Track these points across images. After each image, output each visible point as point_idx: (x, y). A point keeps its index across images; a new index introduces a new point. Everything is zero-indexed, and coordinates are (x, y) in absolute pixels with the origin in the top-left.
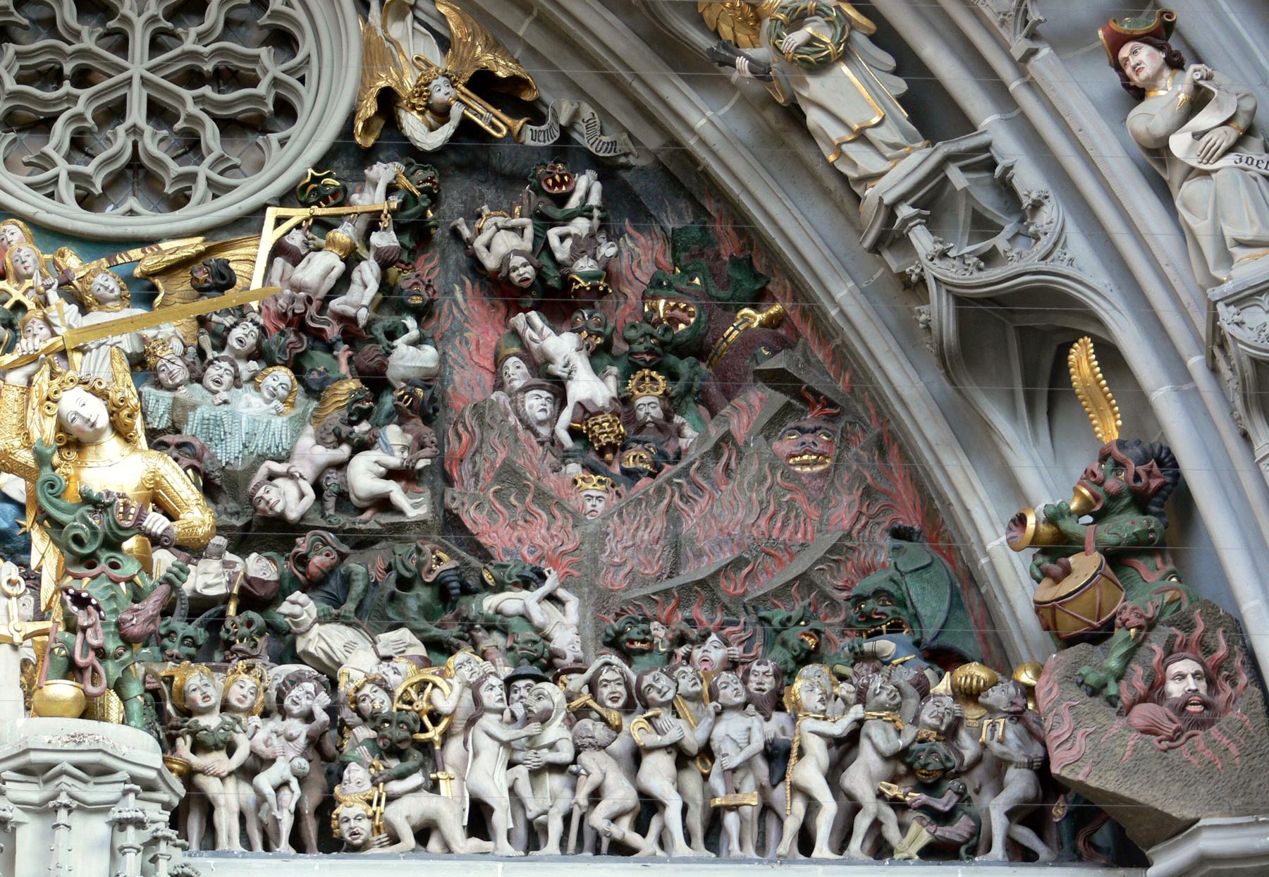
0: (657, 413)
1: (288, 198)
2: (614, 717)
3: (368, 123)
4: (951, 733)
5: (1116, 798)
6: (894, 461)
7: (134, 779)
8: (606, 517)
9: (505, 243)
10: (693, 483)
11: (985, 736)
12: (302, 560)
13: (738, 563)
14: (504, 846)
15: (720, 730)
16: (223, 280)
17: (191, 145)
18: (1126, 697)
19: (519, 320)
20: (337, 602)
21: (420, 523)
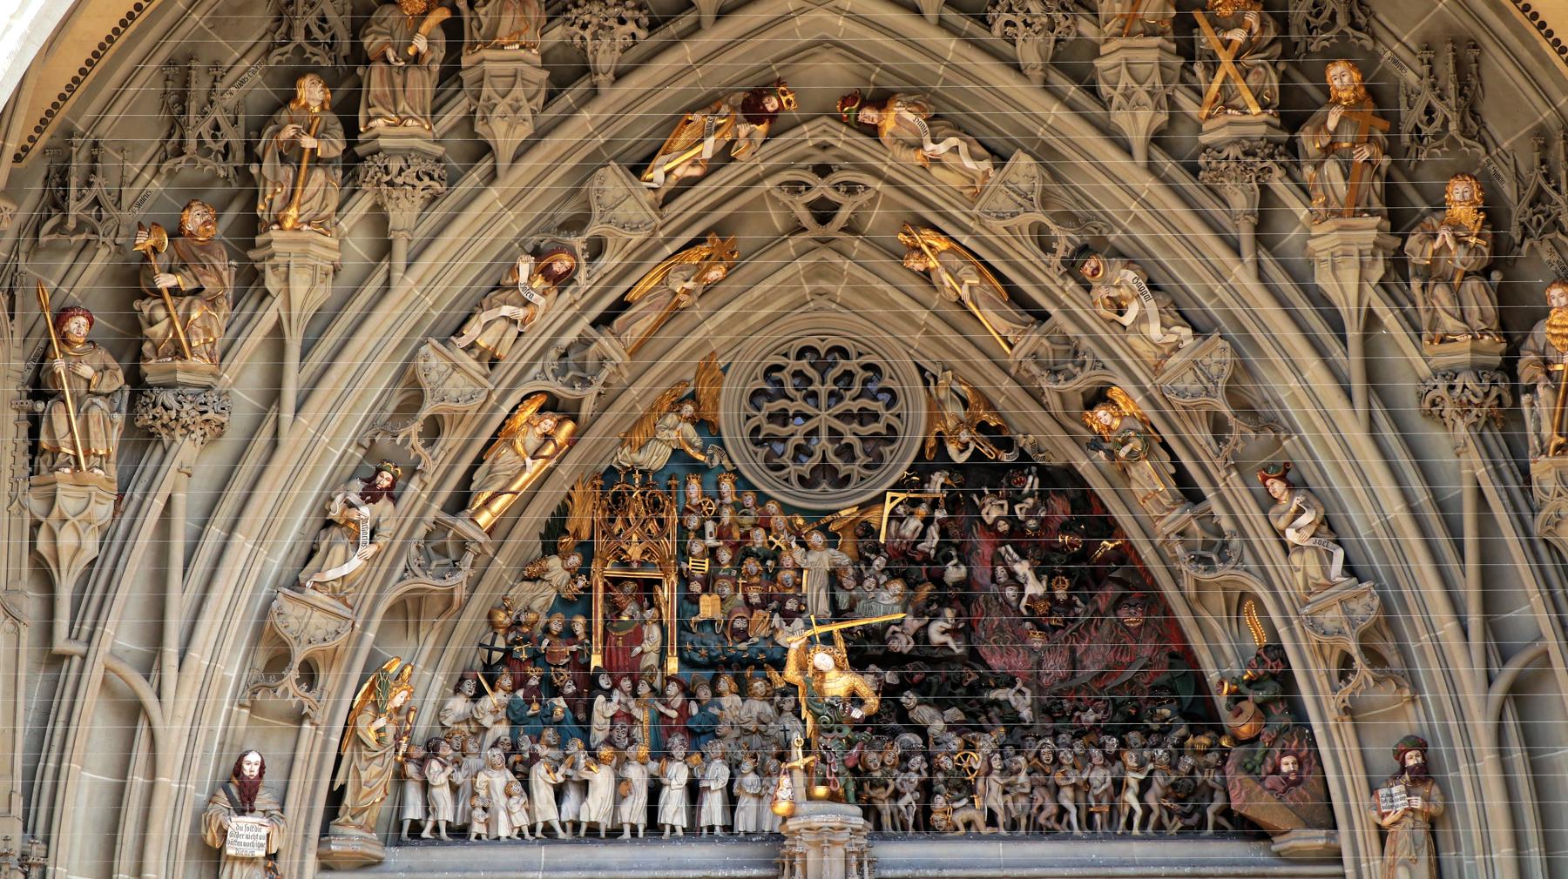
1: (896, 487)
2: (1048, 770)
3: (931, 449)
9: (995, 514)
16: (870, 531)
21: (960, 656)
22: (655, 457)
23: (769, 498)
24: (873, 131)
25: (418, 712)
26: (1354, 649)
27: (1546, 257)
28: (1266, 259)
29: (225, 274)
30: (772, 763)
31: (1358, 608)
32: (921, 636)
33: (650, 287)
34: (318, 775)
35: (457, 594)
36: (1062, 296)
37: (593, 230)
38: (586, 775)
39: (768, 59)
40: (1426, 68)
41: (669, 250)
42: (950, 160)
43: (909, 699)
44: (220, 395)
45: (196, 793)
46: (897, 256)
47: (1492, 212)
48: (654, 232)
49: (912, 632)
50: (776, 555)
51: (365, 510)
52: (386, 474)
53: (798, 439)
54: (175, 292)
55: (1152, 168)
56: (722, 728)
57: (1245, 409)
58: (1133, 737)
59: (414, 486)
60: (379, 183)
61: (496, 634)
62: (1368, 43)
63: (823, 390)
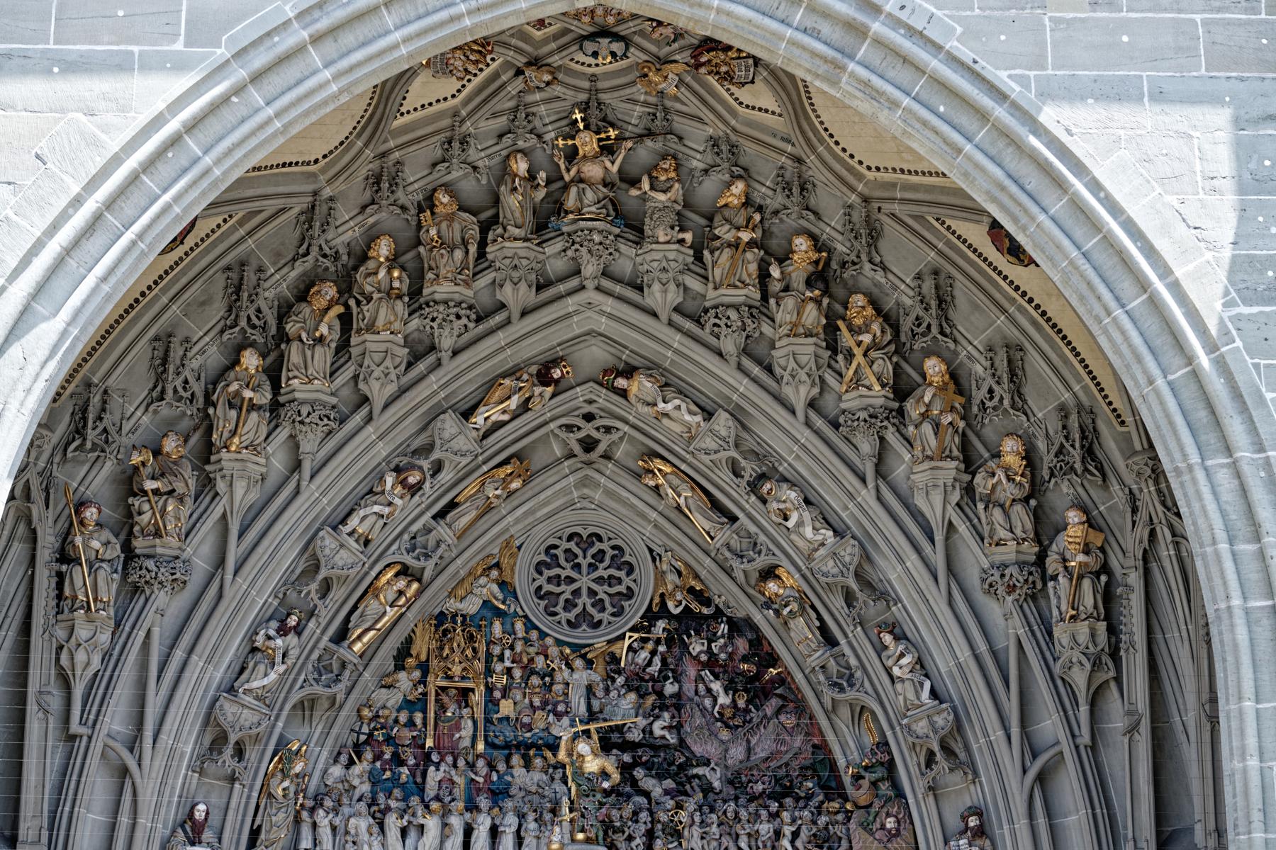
1: (631, 630)
12: (640, 757)
16: (615, 659)
20: (649, 769)
22: (471, 606)
23: (547, 635)
24: (623, 393)
25: (310, 776)
26: (936, 748)
27: (1065, 490)
28: (880, 482)
29: (190, 481)
30: (548, 816)
31: (940, 721)
32: (647, 731)
34: (244, 816)
37: (436, 455)
38: (422, 821)
39: (555, 343)
40: (989, 363)
41: (485, 468)
42: (674, 414)
44: (184, 562)
45: (162, 831)
46: (638, 476)
47: (1030, 457)
48: (476, 456)
50: (551, 674)
51: (279, 642)
52: (294, 617)
53: (567, 595)
54: (156, 492)
55: (808, 424)
56: (513, 791)
57: (866, 583)
58: (788, 801)
59: (312, 624)
60: (294, 421)
62: (952, 345)
63: (584, 563)
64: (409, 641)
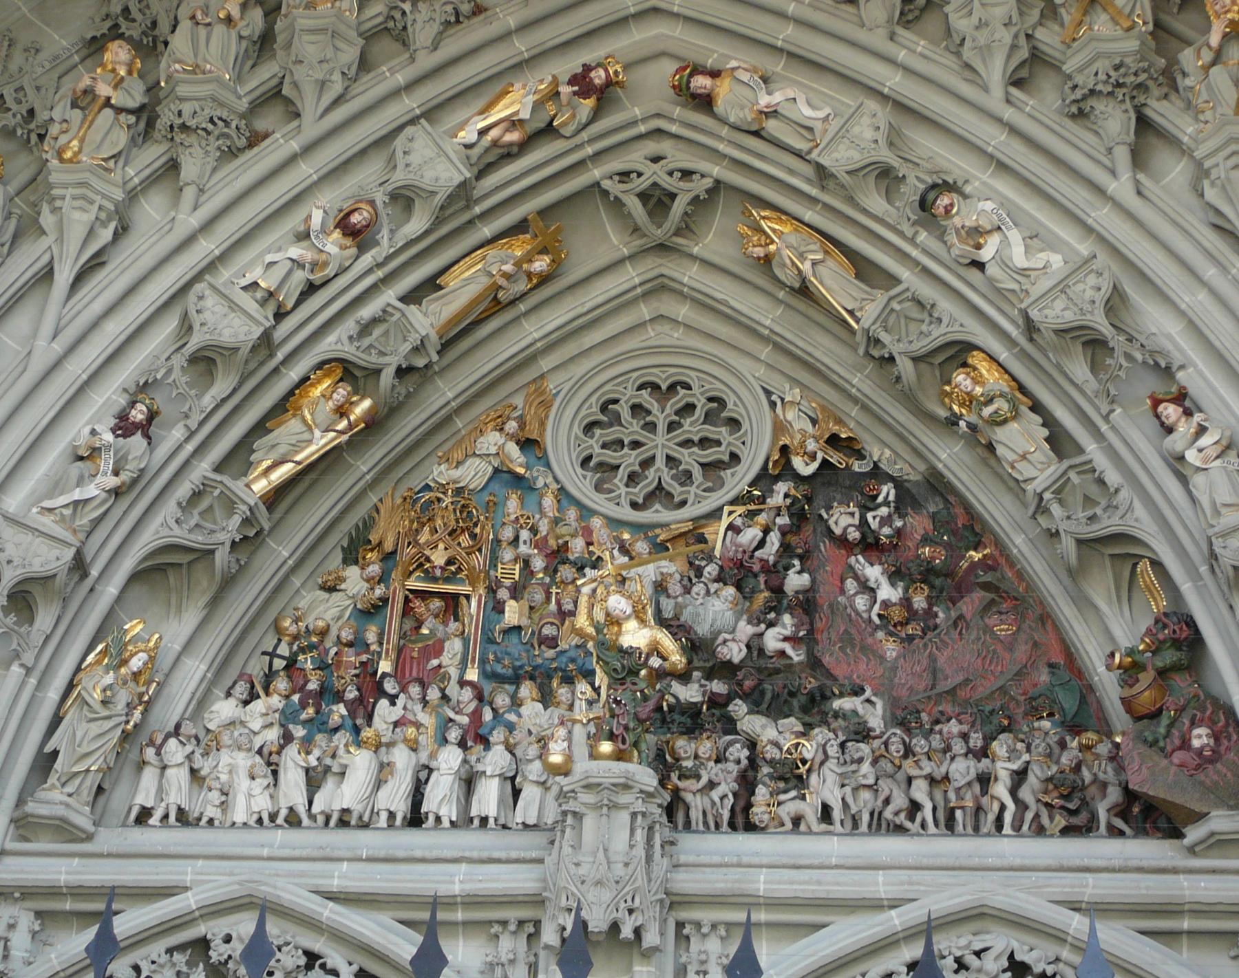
0: (924, 605)
1: (733, 502)
2: (897, 762)
4: (1077, 769)
5: (1164, 800)
6: (1049, 627)
7: (642, 792)
8: (897, 658)
9: (845, 521)
10: (941, 640)
11: (1095, 769)
12: (740, 684)
13: (967, 681)
14: (838, 827)
15: (954, 766)
17: (688, 475)
18: (1169, 748)
19: (852, 560)
21: (800, 663)
22: (473, 473)
23: (594, 513)
32: (755, 646)
33: (467, 274)
35: (218, 555)
36: (915, 253)
41: (487, 231)
43: (739, 708)
49: (745, 639)
52: (140, 406)
59: (178, 433)
61: (280, 640)
64: (368, 524)
